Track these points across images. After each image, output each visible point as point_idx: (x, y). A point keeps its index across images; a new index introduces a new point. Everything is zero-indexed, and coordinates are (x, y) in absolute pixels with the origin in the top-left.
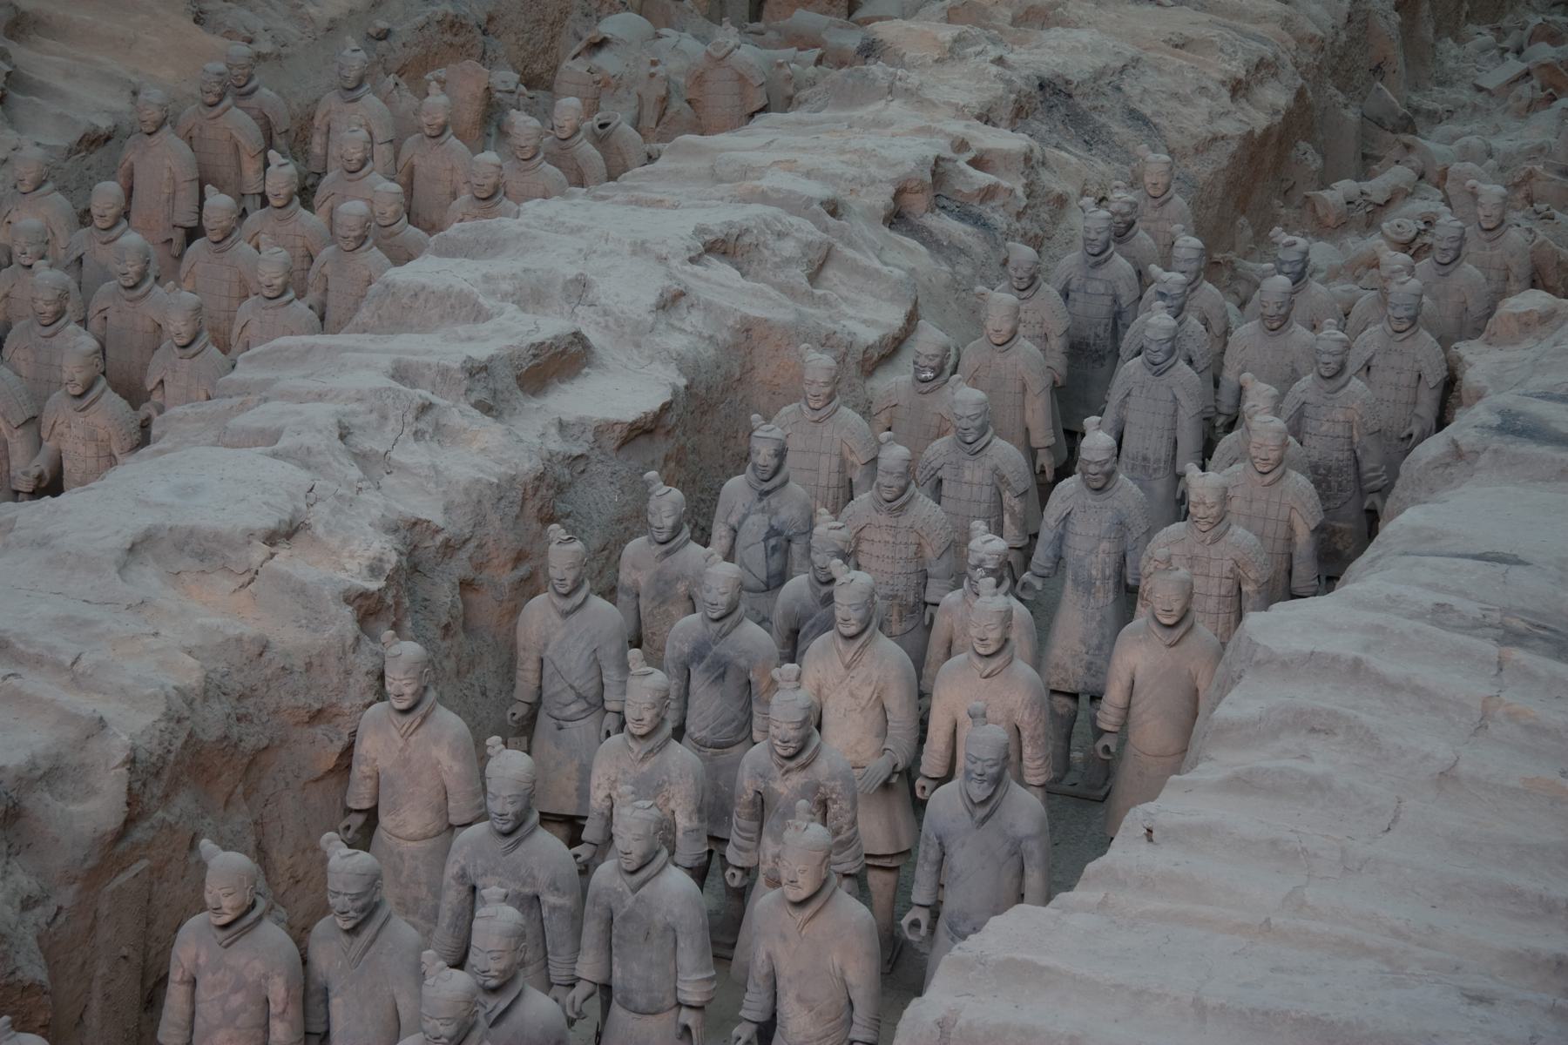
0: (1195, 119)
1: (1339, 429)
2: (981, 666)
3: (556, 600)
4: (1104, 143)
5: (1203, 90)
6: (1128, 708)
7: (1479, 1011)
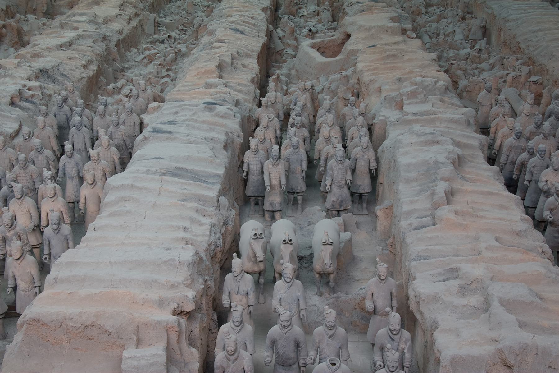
0: (77, 74)
1: (120, 137)
2: (51, 200)
4: (57, 82)
5: (77, 68)
6: (85, 203)
7: (168, 251)
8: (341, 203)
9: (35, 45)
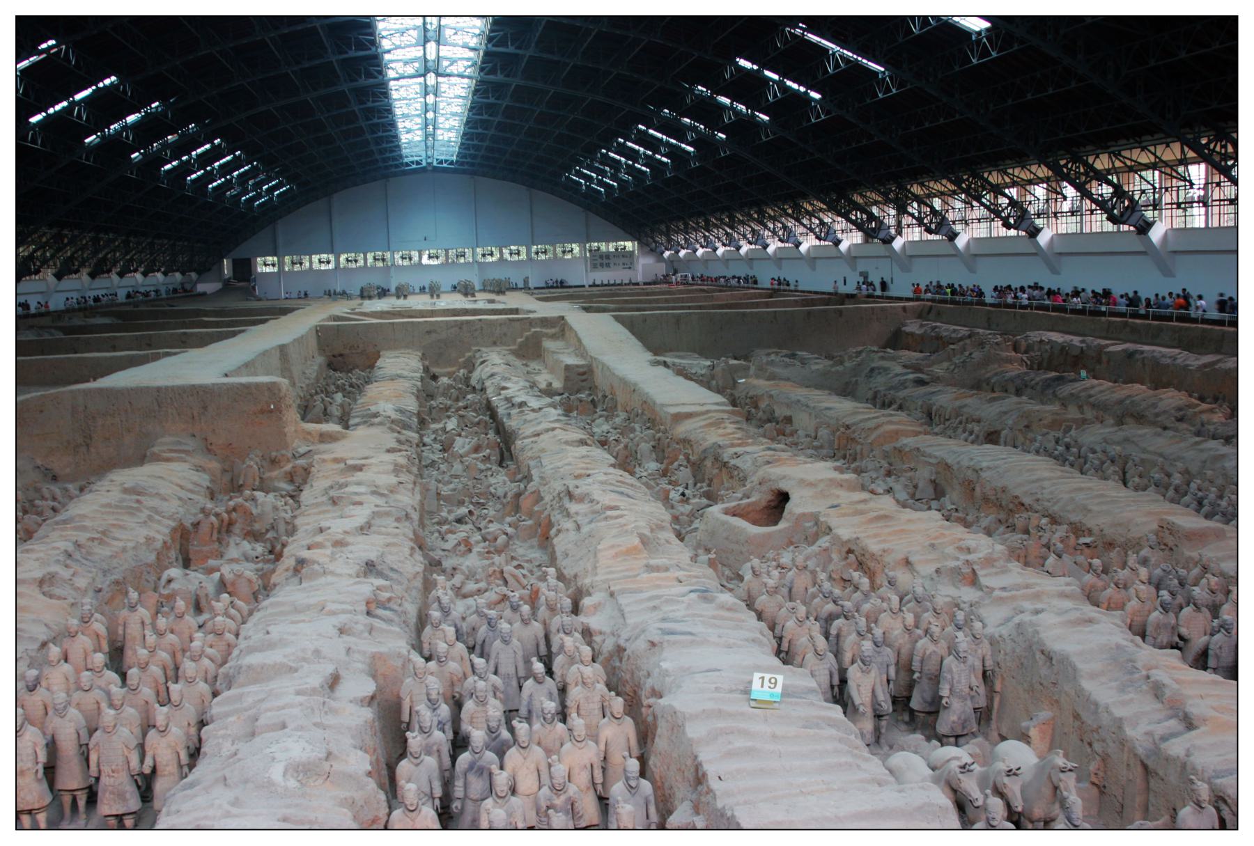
3: (413, 760)
6: (606, 752)
8: (964, 725)
9: (321, 530)
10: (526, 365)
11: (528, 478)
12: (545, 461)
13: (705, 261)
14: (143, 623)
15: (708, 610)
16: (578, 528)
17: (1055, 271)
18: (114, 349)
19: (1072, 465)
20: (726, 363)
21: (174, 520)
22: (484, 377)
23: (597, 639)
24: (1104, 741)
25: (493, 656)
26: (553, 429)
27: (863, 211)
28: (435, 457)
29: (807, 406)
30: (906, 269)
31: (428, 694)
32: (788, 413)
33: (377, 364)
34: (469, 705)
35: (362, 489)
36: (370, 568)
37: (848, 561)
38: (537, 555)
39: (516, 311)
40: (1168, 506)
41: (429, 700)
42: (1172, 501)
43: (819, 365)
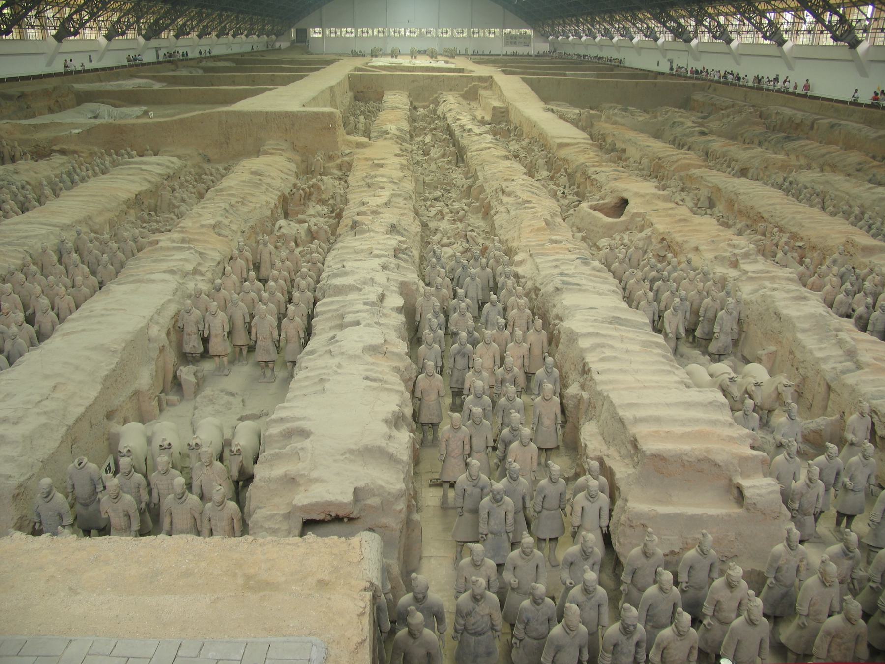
9: (364, 204)
10: (469, 104)
11: (475, 177)
12: (486, 168)
13: (574, 45)
14: (271, 253)
15: (586, 270)
16: (508, 212)
17: (790, 68)
18: (233, 83)
19: (793, 196)
20: (588, 112)
21: (280, 191)
22: (445, 111)
23: (523, 280)
24: (806, 368)
25: (465, 286)
26: (489, 148)
27: (675, 21)
28: (419, 159)
29: (636, 143)
30: (697, 59)
31: (434, 309)
32: (624, 146)
33: (384, 99)
34: (454, 316)
35: (385, 179)
36: (393, 229)
37: (663, 245)
38: (482, 223)
39: (462, 70)
40: (851, 228)
41: (434, 312)
42: (852, 224)
43: (642, 117)
